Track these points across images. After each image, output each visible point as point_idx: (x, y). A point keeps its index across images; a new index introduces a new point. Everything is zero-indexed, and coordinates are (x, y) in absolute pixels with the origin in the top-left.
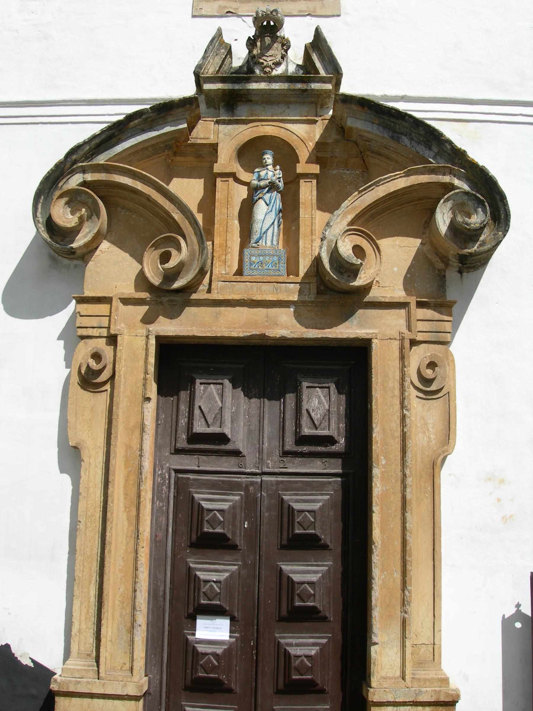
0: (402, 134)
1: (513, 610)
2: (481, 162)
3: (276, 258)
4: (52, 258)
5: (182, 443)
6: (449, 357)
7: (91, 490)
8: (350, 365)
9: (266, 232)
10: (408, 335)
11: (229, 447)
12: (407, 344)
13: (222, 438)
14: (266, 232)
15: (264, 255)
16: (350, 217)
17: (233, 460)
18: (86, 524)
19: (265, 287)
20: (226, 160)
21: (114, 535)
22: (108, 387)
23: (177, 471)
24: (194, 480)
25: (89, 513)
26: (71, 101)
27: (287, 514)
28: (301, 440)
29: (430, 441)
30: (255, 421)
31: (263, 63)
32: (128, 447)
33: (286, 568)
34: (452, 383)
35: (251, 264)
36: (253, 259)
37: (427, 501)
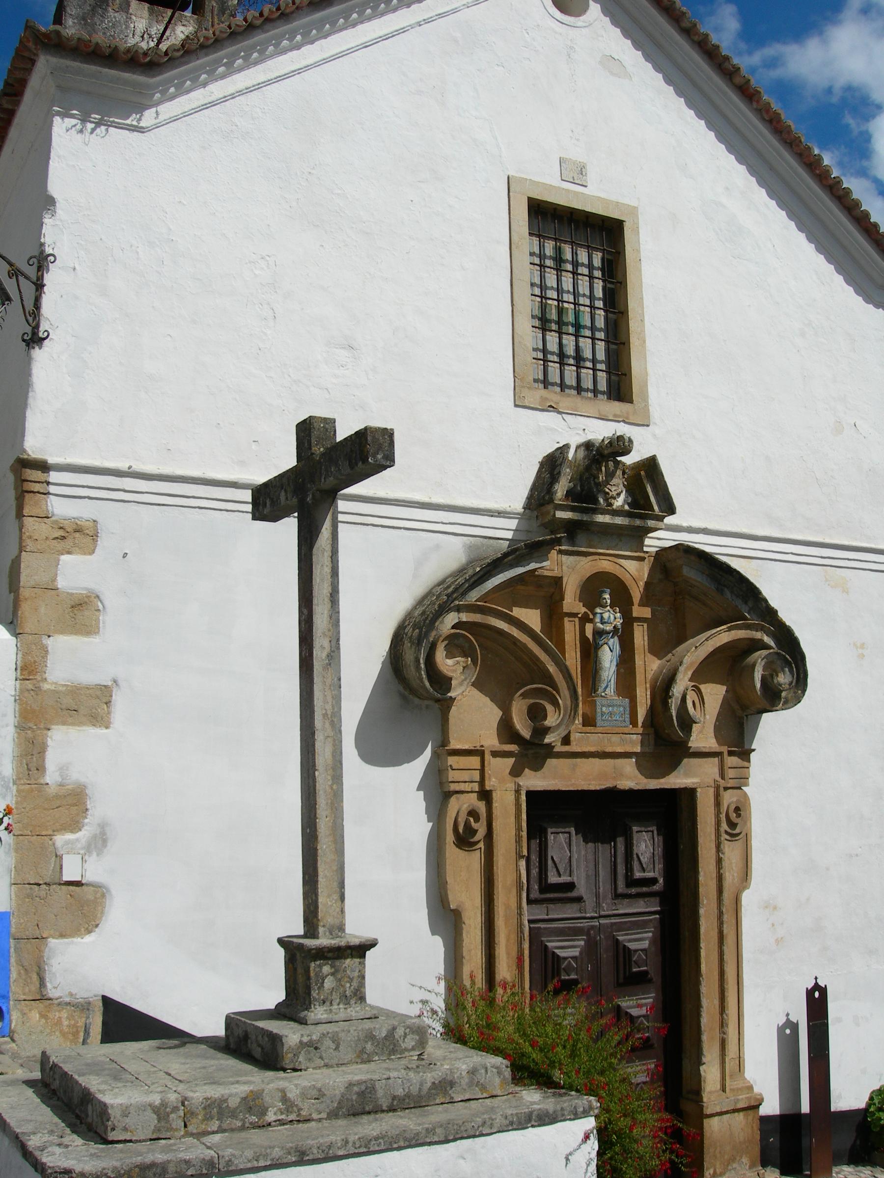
0: (725, 586)
1: (784, 1020)
3: (622, 709)
4: (404, 697)
5: (535, 894)
8: (673, 813)
15: (613, 706)
16: (690, 673)
17: (576, 906)
24: (545, 928)
26: (403, 501)
27: (623, 954)
28: (631, 882)
30: (592, 866)
31: (608, 493)
32: (507, 907)
35: (602, 715)
36: (604, 709)
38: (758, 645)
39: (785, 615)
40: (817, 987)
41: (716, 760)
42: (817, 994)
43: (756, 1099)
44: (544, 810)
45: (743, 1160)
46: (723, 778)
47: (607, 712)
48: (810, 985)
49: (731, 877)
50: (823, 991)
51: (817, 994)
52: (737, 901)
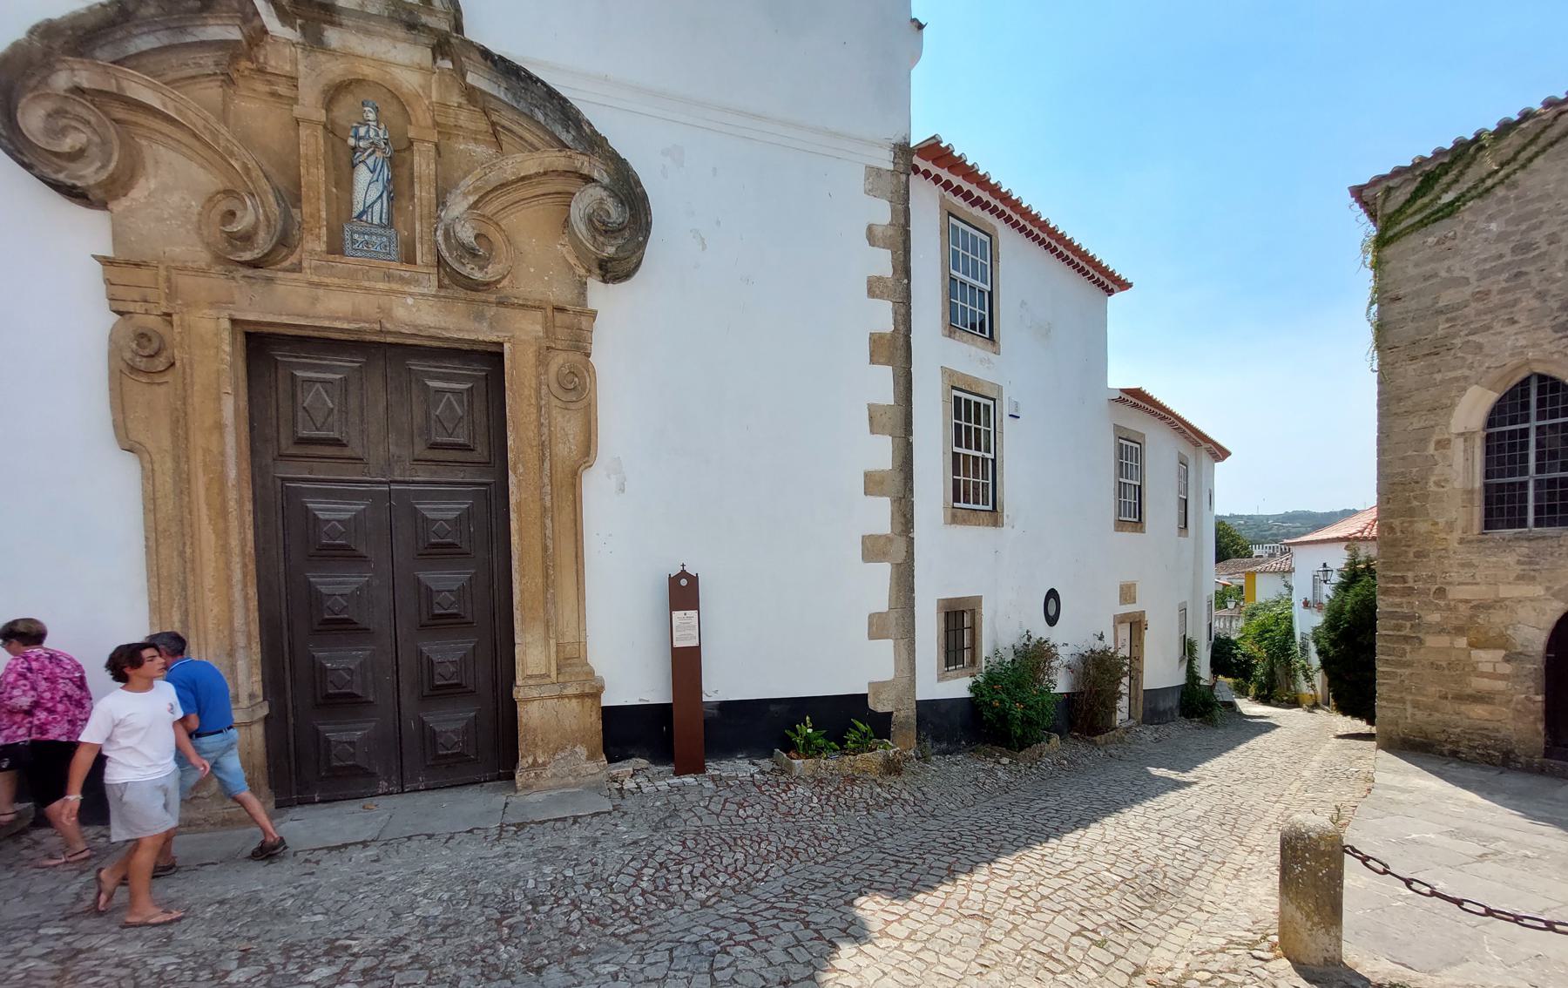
6: (588, 367)
7: (159, 501)
10: (545, 343)
11: (347, 452)
13: (337, 443)
16: (472, 199)
23: (283, 479)
33: (421, 575)
37: (568, 509)
38: (588, 179)
40: (683, 574)
41: (539, 314)
42: (684, 582)
44: (262, 348)
48: (677, 571)
49: (566, 449)
50: (694, 581)
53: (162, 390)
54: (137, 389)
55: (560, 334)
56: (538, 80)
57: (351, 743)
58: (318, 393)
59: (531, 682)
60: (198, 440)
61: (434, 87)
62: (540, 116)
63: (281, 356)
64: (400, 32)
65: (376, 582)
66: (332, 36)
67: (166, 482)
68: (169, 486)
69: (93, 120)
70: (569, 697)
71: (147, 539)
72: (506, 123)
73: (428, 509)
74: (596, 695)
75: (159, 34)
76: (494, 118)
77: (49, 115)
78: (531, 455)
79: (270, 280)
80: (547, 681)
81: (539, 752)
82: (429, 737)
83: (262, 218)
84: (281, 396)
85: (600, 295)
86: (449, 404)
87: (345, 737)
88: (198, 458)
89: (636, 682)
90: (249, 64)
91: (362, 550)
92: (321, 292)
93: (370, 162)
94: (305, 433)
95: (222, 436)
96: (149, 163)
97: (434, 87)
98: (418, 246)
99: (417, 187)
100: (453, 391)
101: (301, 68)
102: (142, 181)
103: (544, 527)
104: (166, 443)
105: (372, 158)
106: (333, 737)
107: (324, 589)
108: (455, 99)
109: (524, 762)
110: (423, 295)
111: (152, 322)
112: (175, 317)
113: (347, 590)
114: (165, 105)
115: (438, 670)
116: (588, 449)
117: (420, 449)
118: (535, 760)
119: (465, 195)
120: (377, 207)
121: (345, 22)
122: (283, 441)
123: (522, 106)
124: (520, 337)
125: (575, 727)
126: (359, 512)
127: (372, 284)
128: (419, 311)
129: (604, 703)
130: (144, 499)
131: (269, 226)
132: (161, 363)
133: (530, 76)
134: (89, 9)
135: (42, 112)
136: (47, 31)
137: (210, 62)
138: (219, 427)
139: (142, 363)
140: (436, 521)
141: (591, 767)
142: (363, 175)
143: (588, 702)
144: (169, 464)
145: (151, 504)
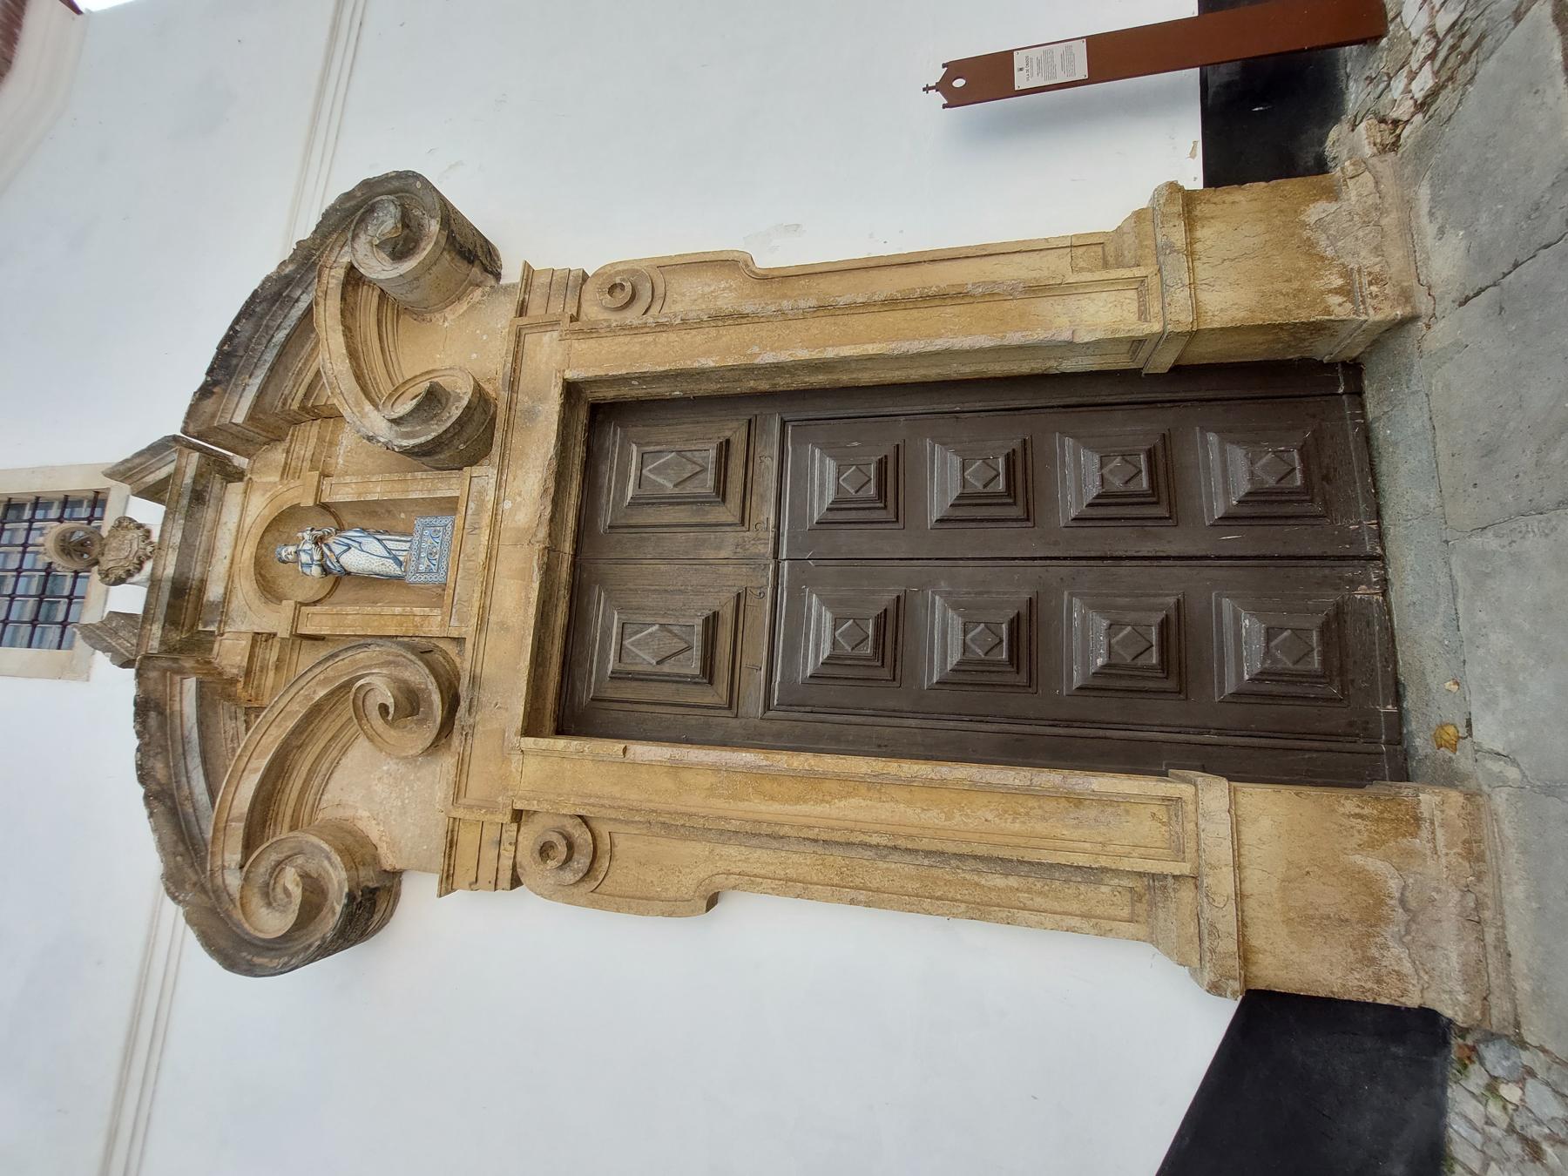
2: (315, 218)
7: (791, 872)
9: (389, 551)
11: (727, 615)
12: (576, 326)
13: (712, 622)
14: (389, 551)
15: (420, 549)
16: (368, 407)
18: (857, 888)
19: (468, 548)
20: (277, 620)
21: (878, 827)
22: (603, 830)
23: (767, 707)
25: (836, 880)
29: (730, 289)
32: (712, 791)
34: (645, 264)
35: (430, 571)
36: (422, 568)
39: (306, 228)
40: (943, 86)
41: (530, 339)
42: (959, 83)
43: (1170, 200)
45: (1312, 220)
46: (557, 323)
47: (426, 562)
48: (938, 98)
49: (725, 294)
51: (959, 83)
52: (767, 279)
53: (622, 844)
54: (621, 874)
55: (556, 307)
56: (232, 328)
57: (1270, 634)
58: (637, 644)
59: (1155, 307)
60: (695, 802)
61: (265, 479)
62: (281, 336)
63: (586, 695)
64: (209, 514)
65: (944, 586)
66: (214, 592)
67: (761, 859)
68: (765, 855)
69: (274, 857)
70: (1191, 242)
71: (852, 902)
72: (302, 391)
73: (820, 501)
74: (1189, 199)
75: (190, 767)
76: (295, 406)
77: (269, 904)
78: (731, 335)
79: (474, 680)
80: (1154, 281)
81: (1318, 285)
82: (1261, 507)
83: (385, 671)
84: (643, 697)
85: (511, 273)
86: (656, 471)
87: (1258, 645)
88: (720, 805)
89: (1166, 143)
90: (240, 686)
91: (886, 599)
92: (493, 618)
93: (337, 549)
94: (694, 668)
95: (689, 767)
96: (341, 813)
97: (265, 479)
98: (439, 494)
99: (369, 498)
100: (642, 464)
101: (243, 629)
102: (360, 825)
103: (852, 308)
104: (699, 849)
105: (334, 547)
106: (1252, 665)
107: (954, 658)
108: (278, 455)
109: (1340, 308)
110: (498, 486)
111: (530, 837)
112: (518, 806)
113: (956, 622)
114: (256, 770)
115: (1117, 484)
116: (727, 264)
117: (728, 512)
118: (1338, 291)
119: (363, 415)
120: (390, 545)
121: (197, 575)
122: (708, 700)
123: (269, 357)
124: (554, 360)
125: (1261, 228)
126: (823, 601)
127: (483, 549)
128: (518, 490)
129: (1199, 185)
130: (785, 894)
131: (396, 664)
132: (581, 836)
133: (229, 338)
134: (155, 830)
135: (264, 911)
136: (174, 883)
137: (230, 724)
138: (675, 767)
139: (581, 862)
140: (839, 488)
141: (1357, 193)
142: (355, 560)
143: (1201, 210)
144: (732, 851)
145: (794, 886)
